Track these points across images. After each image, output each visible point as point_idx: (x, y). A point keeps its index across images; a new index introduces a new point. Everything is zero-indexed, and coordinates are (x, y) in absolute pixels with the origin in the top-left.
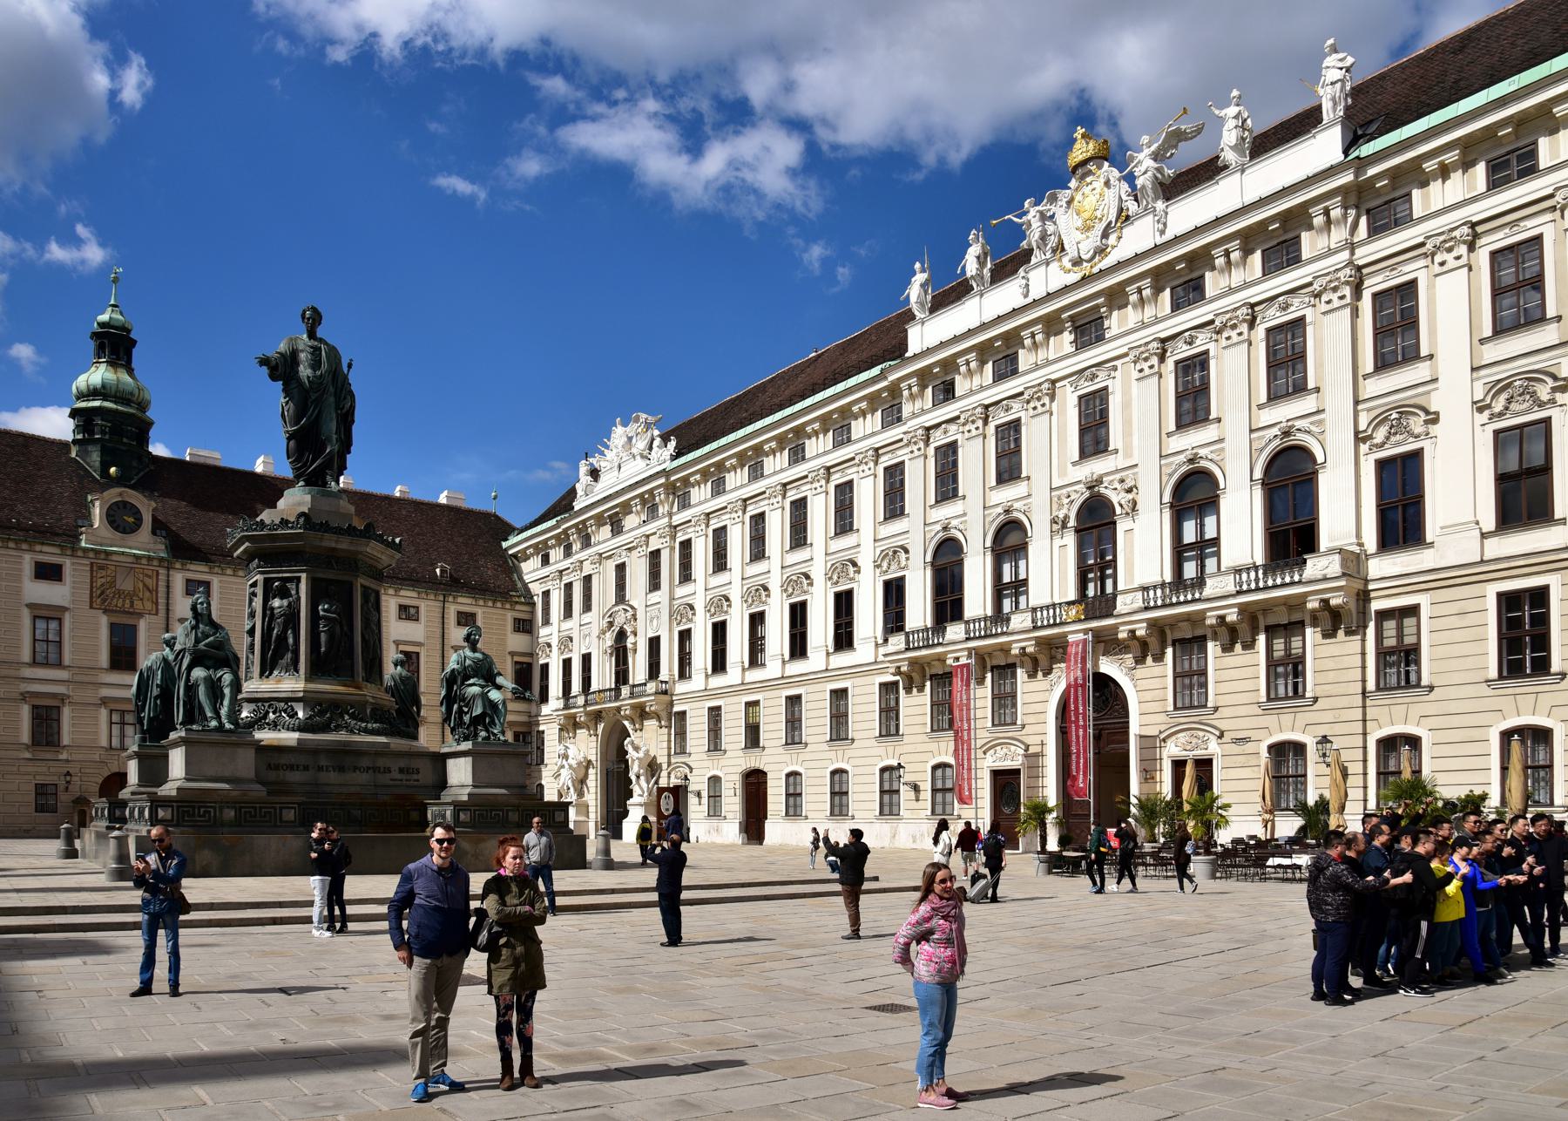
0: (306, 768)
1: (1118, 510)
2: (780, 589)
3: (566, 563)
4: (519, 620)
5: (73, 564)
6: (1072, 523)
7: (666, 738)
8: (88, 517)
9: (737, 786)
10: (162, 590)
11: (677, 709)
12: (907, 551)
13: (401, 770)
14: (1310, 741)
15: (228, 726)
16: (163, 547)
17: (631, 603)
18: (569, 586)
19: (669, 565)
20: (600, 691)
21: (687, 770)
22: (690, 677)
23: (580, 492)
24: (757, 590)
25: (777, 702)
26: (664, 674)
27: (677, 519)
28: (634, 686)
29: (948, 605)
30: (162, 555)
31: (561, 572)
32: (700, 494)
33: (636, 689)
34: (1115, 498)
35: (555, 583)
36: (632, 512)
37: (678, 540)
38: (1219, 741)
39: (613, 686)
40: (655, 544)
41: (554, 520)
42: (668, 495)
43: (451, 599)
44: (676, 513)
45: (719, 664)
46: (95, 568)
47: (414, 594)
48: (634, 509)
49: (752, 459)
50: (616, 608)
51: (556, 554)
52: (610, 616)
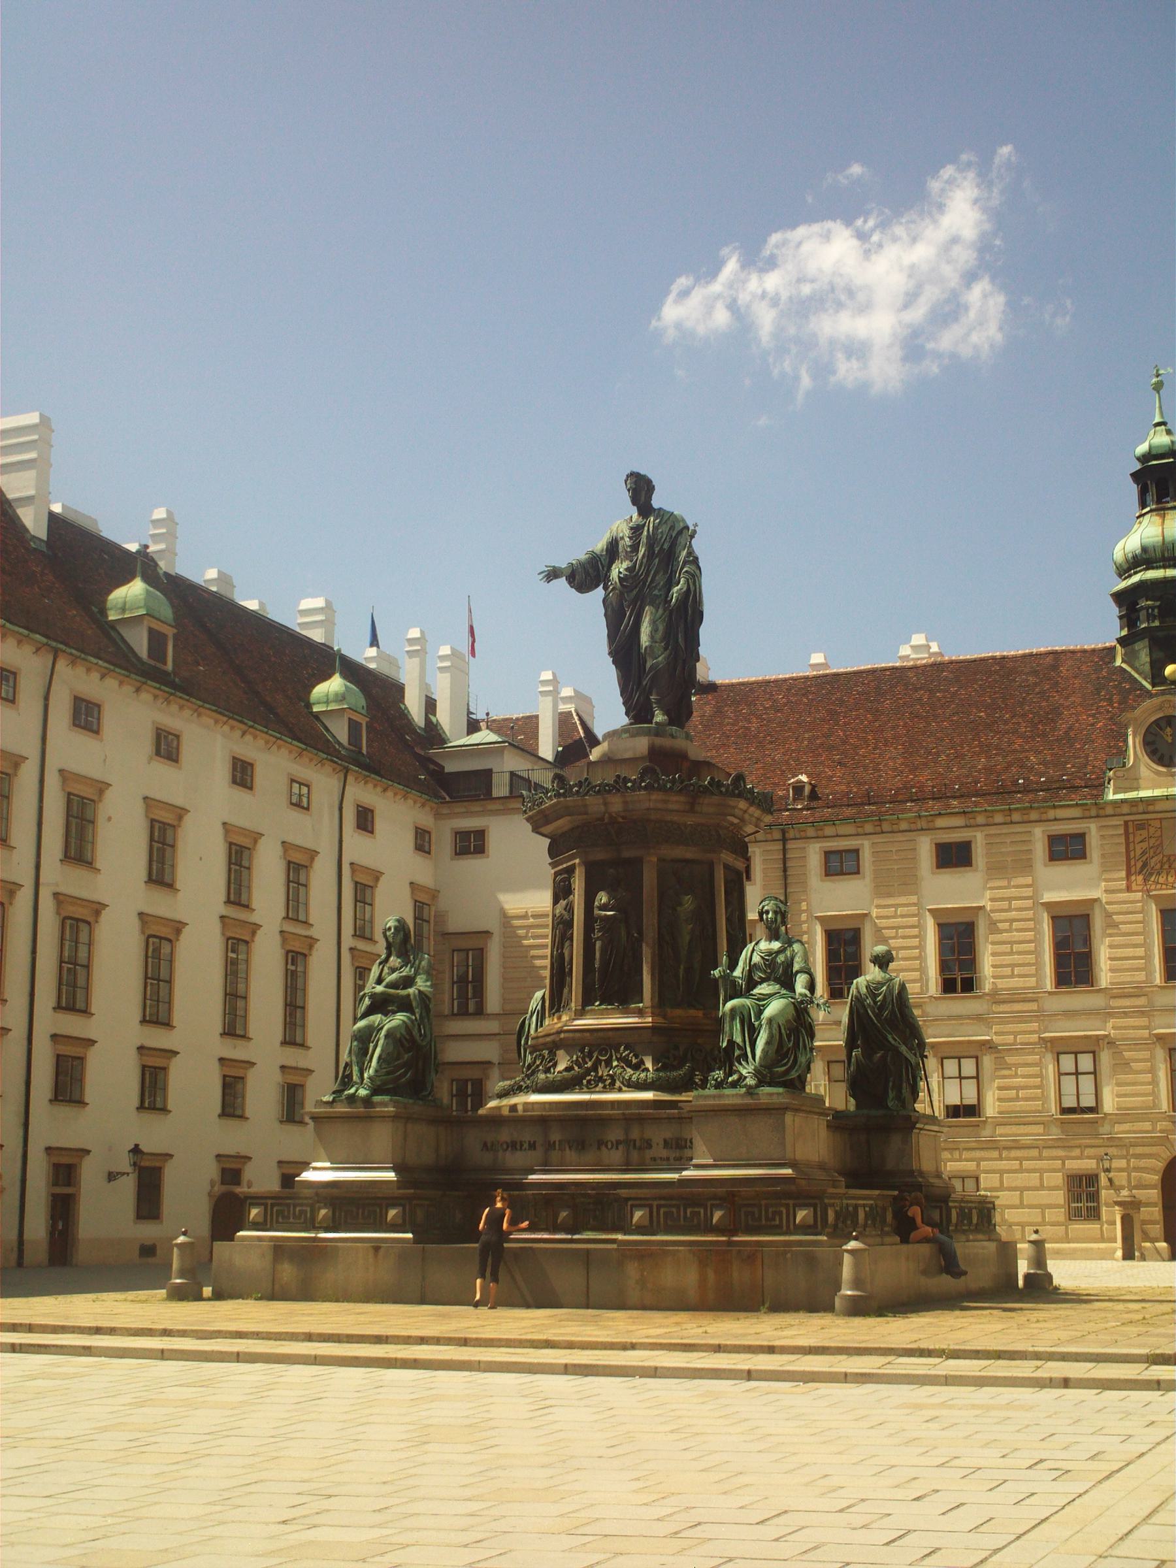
0: (532, 1146)
46: (1131, 830)
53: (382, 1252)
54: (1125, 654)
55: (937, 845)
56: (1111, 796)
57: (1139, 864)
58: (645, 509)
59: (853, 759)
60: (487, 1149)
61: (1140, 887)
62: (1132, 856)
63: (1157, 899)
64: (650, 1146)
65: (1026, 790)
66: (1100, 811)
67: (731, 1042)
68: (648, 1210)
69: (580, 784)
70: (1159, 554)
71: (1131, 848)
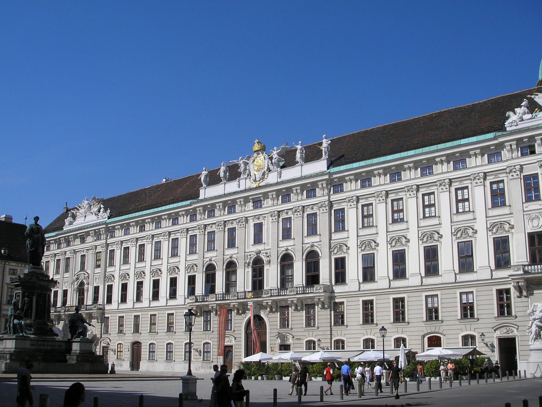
0: (35, 345)
1: (265, 263)
2: (150, 274)
3: (59, 251)
6: (251, 265)
7: (100, 327)
9: (129, 348)
11: (106, 316)
12: (197, 266)
13: (58, 346)
14: (316, 340)
18: (59, 261)
21: (109, 340)
23: (67, 223)
24: (141, 273)
25: (146, 316)
26: (100, 301)
27: (110, 241)
28: (87, 305)
29: (210, 288)
34: (265, 259)
35: (52, 258)
36: (90, 235)
38: (293, 339)
41: (56, 233)
42: (106, 231)
43: (7, 263)
44: (109, 239)
45: (124, 299)
48: (91, 235)
49: (141, 224)
52: (77, 276)
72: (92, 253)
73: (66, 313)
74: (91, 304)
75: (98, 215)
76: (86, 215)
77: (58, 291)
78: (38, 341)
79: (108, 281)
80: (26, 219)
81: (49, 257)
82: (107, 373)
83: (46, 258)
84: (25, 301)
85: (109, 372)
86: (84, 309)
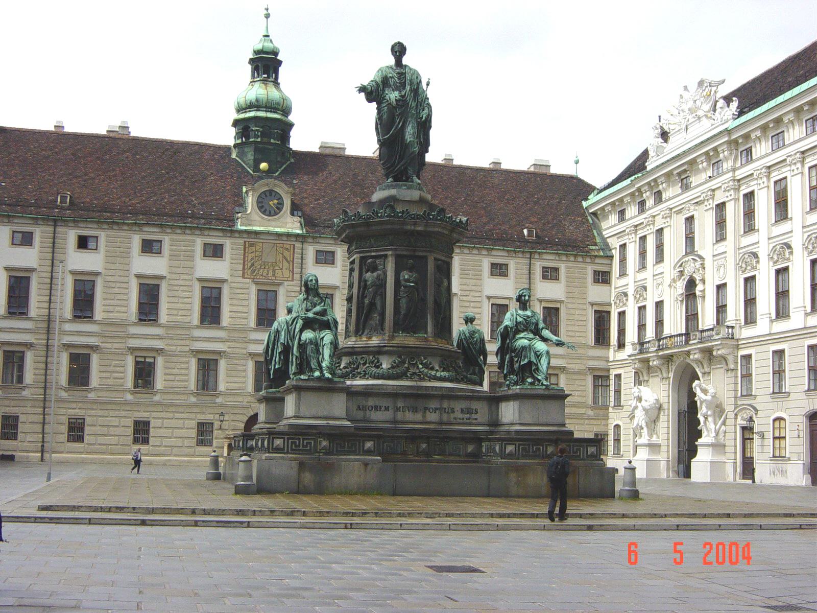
0: (387, 409)
4: (599, 272)
5: (232, 244)
8: (241, 204)
9: (801, 428)
10: (297, 261)
15: (327, 375)
16: (299, 225)
17: (699, 253)
18: (643, 239)
19: (734, 214)
20: (671, 337)
21: (753, 413)
22: (755, 322)
23: (651, 153)
27: (740, 174)
28: (702, 331)
30: (299, 231)
31: (636, 226)
32: (761, 149)
33: (705, 334)
37: (742, 193)
39: (684, 332)
40: (720, 198)
43: (537, 256)
44: (739, 168)
46: (247, 246)
47: (505, 254)
50: (686, 259)
51: (632, 211)
52: (681, 266)
53: (369, 467)
54: (238, 153)
55: (143, 240)
56: (240, 227)
57: (250, 264)
58: (399, 62)
59: (92, 185)
60: (360, 410)
61: (249, 277)
62: (246, 259)
63: (257, 283)
64: (453, 412)
65: (193, 216)
66: (232, 232)
67: (530, 363)
68: (514, 446)
69: (403, 212)
70: (264, 105)
71: (246, 255)
72: (706, 208)
73: (660, 354)
74: (711, 327)
75: (714, 117)
76: (687, 126)
77: (644, 307)
78: (394, 395)
79: (746, 269)
80: (577, 162)
81: (624, 236)
82: (612, 496)
83: (619, 240)
84: (366, 281)
85: (617, 495)
86: (696, 341)
